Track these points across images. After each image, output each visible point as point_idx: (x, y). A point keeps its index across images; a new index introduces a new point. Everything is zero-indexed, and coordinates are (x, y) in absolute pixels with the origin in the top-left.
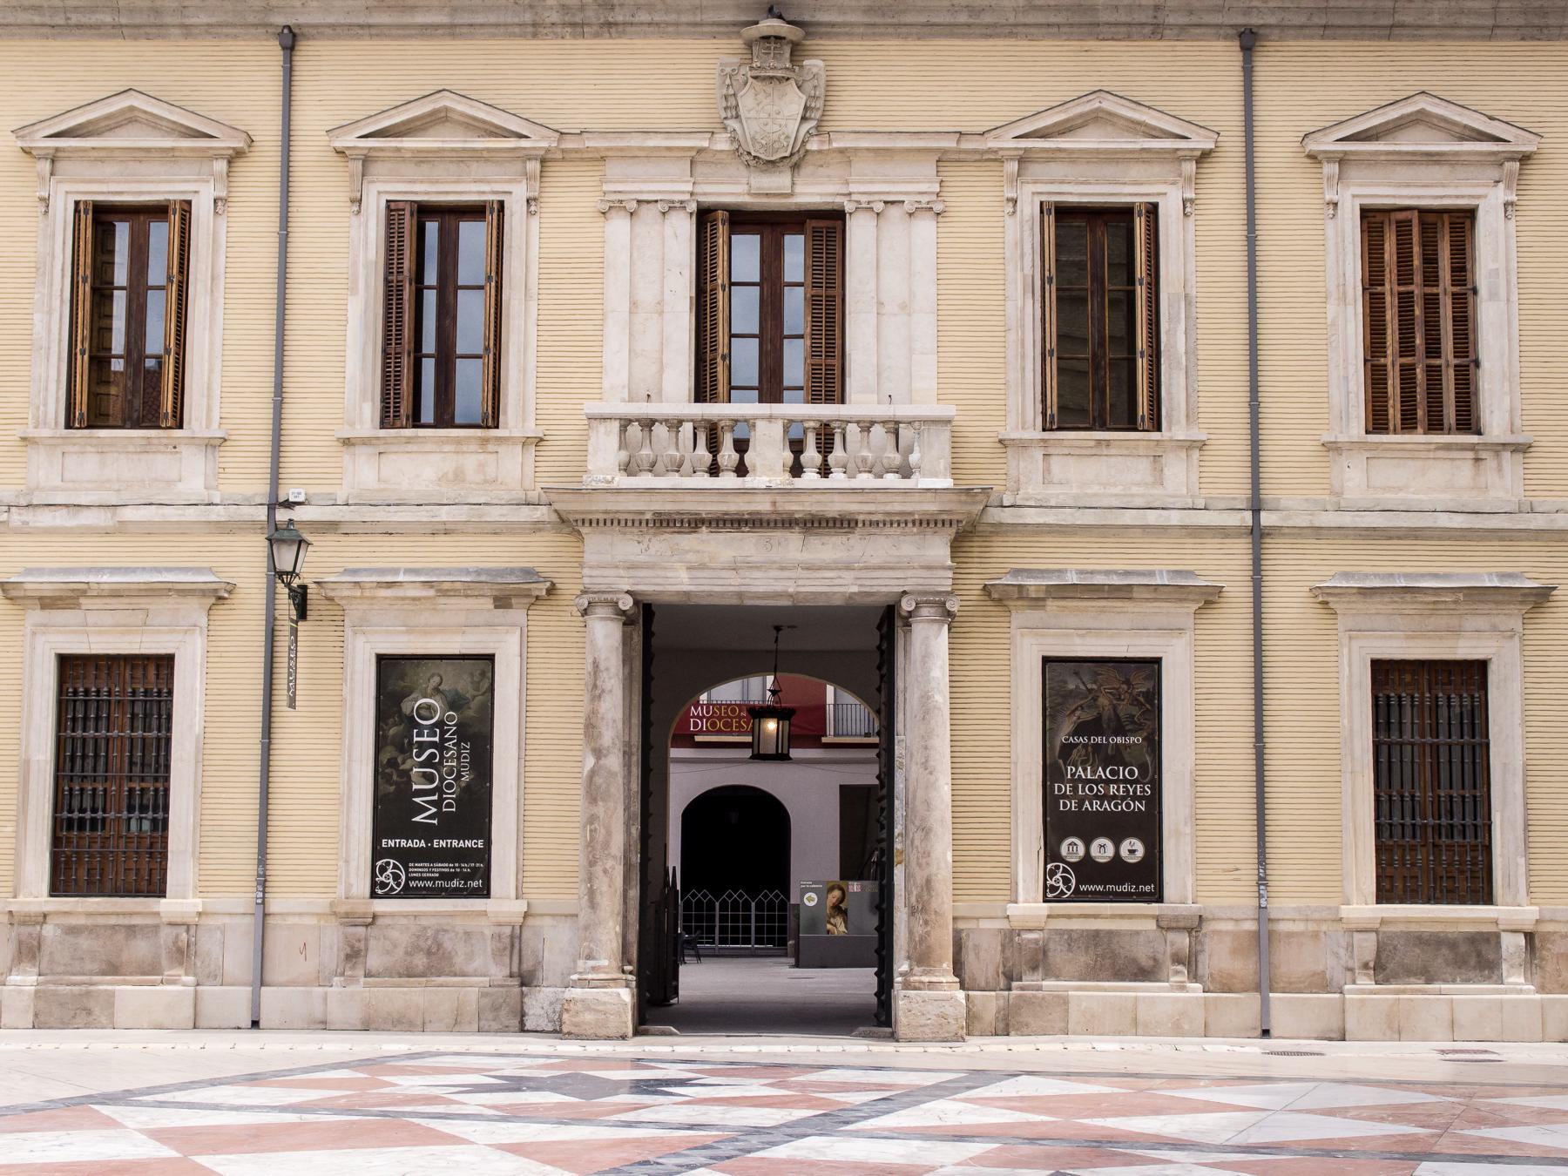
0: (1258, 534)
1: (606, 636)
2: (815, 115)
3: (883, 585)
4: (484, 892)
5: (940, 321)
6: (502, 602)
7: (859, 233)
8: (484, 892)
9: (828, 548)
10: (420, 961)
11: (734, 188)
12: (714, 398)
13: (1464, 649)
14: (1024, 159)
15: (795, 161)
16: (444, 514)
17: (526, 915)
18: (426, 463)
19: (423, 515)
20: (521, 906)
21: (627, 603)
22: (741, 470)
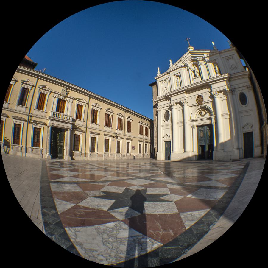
0: (86, 128)
1: (50, 128)
2: (67, 94)
3: (67, 128)
4: (39, 147)
5: (70, 110)
6: (42, 124)
7: (66, 103)
8: (39, 147)
9: (65, 124)
10: (36, 152)
11: (61, 97)
12: (58, 112)
13: (95, 137)
14: (78, 101)
15: (65, 97)
16: (40, 117)
17: (43, 149)
18: (39, 113)
19: (38, 117)
20: (42, 148)
21: (52, 126)
22: (60, 118)
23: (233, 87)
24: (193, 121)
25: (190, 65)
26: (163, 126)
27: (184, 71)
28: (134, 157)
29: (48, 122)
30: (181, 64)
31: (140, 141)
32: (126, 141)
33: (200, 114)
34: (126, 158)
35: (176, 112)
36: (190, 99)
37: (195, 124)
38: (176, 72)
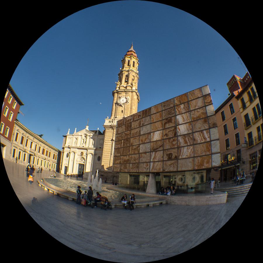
23: (96, 153)
24: (77, 161)
25: (83, 137)
26: (65, 159)
27: (80, 138)
28: (50, 170)
29: (29, 152)
30: (80, 134)
31: (53, 162)
32: (48, 162)
33: (81, 159)
34: (47, 170)
35: (72, 155)
36: (78, 152)
37: (78, 163)
38: (77, 137)
